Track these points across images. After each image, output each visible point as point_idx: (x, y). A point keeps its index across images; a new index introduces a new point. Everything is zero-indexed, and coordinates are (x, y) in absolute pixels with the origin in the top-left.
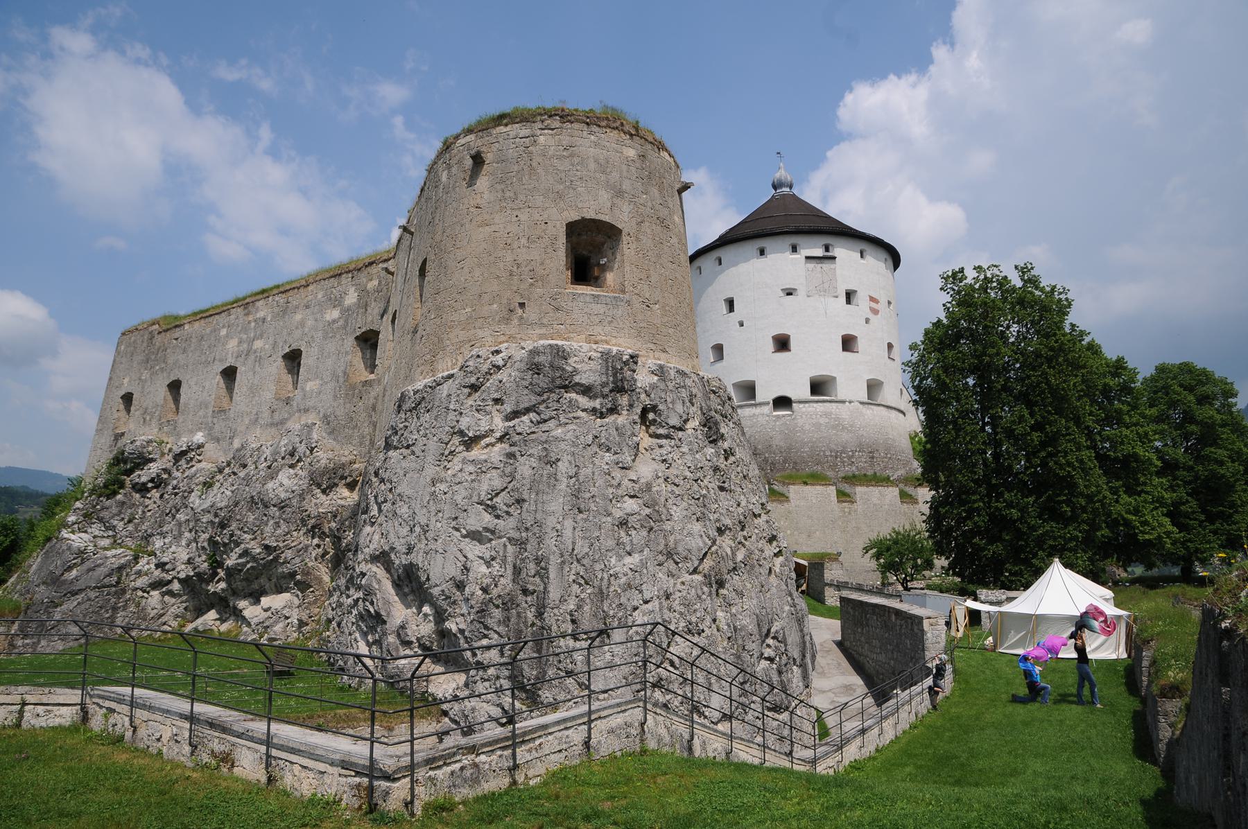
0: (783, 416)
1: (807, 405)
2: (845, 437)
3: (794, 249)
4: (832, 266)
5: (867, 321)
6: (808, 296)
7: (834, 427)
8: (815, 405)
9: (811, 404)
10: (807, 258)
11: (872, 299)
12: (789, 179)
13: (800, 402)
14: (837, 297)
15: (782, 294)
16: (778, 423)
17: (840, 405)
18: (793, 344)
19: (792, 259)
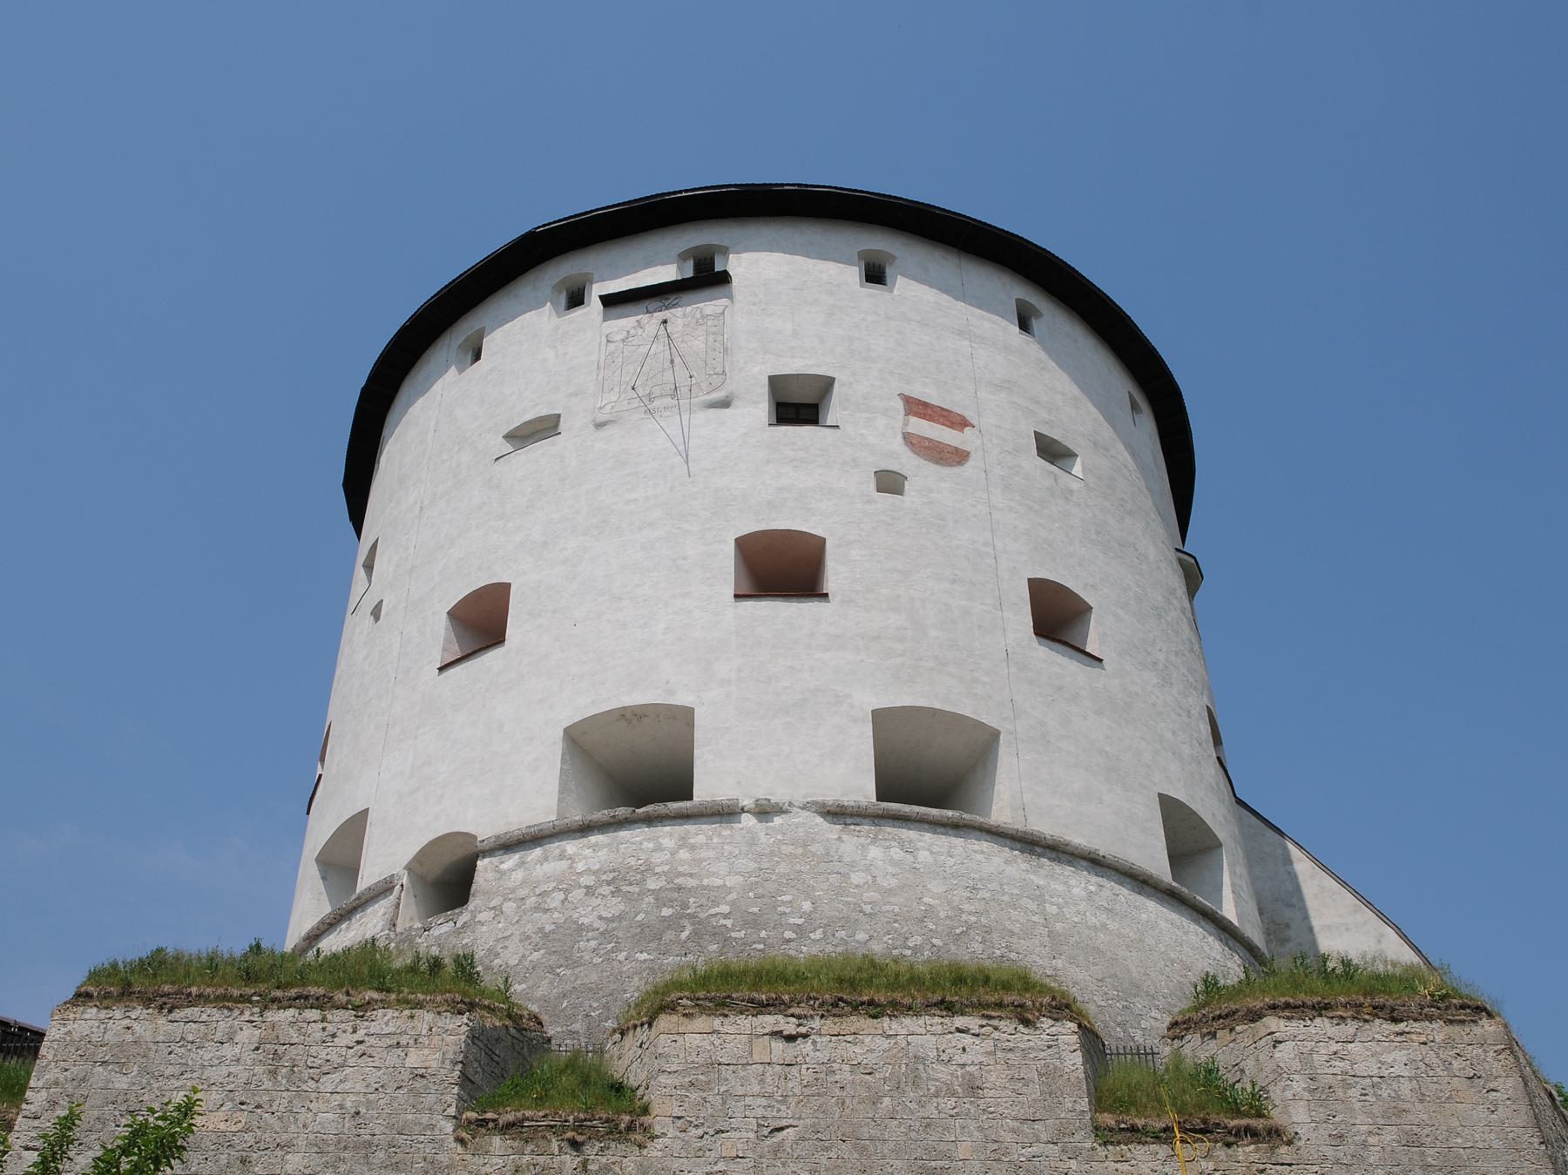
1: (537, 852)
6: (600, 425)
8: (571, 846)
9: (554, 847)
10: (609, 301)
14: (725, 404)
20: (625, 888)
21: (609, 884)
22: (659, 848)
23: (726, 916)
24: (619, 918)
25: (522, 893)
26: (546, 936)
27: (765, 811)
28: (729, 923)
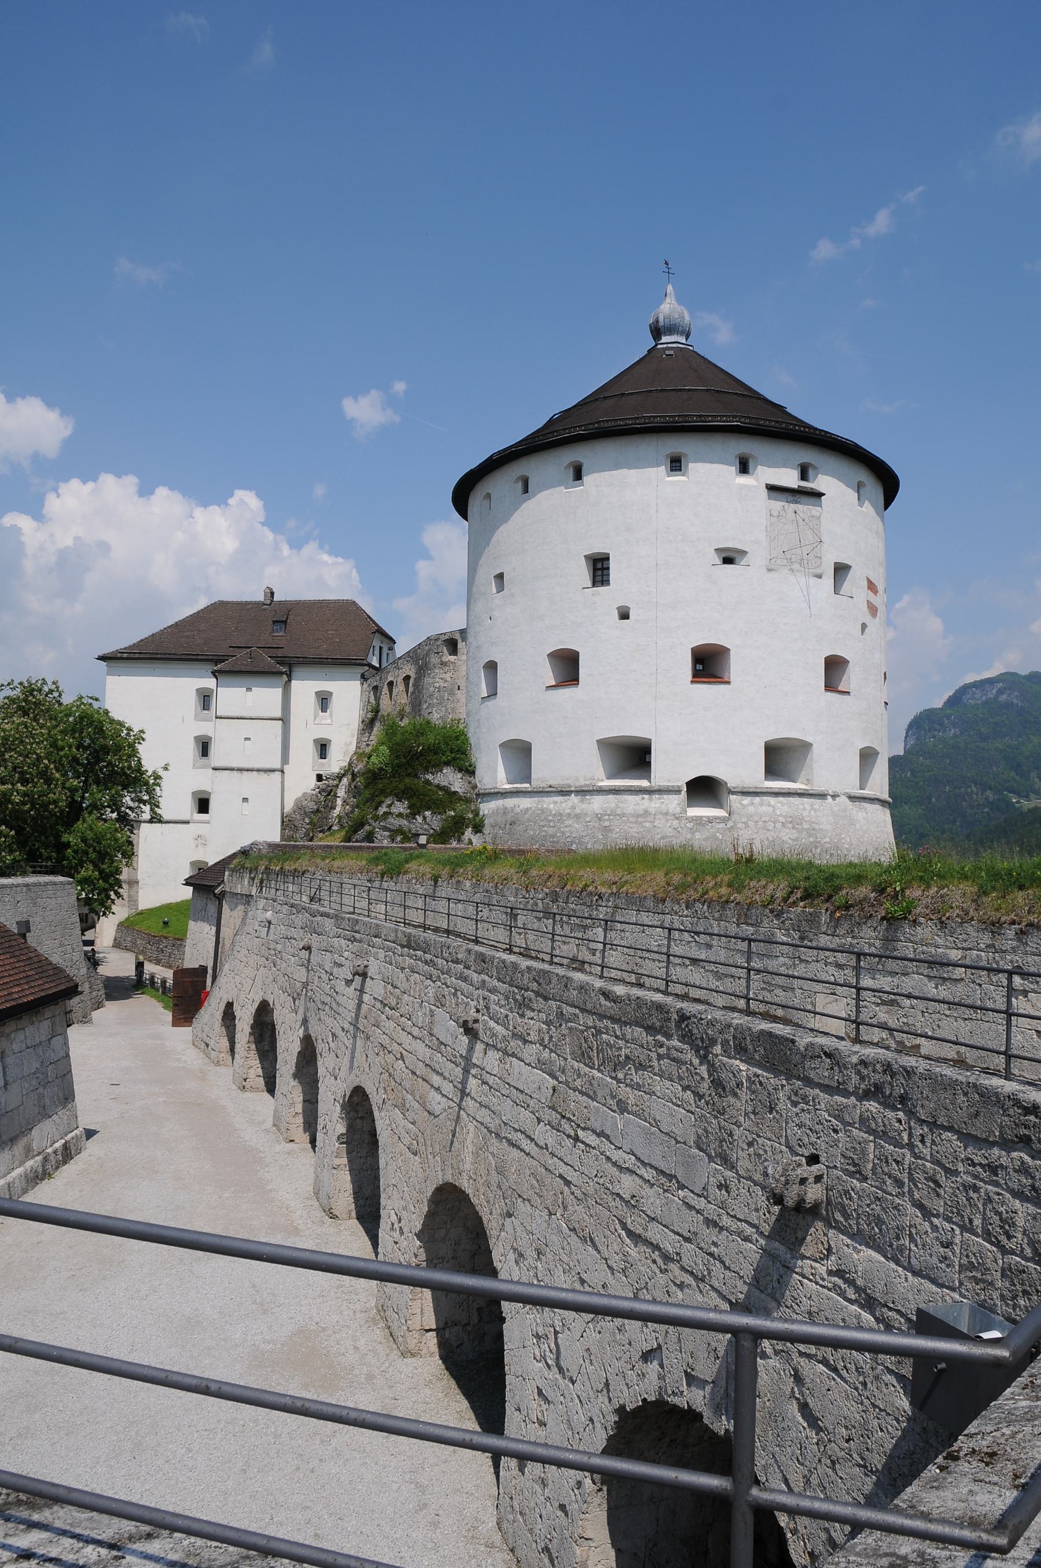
0: (710, 820)
1: (757, 800)
3: (744, 468)
4: (815, 511)
5: (864, 626)
6: (770, 570)
8: (772, 800)
10: (772, 489)
12: (687, 318)
13: (745, 793)
14: (820, 577)
15: (718, 561)
16: (698, 835)
17: (816, 802)
18: (736, 666)
19: (742, 487)
22: (805, 809)
23: (829, 843)
25: (756, 819)
27: (834, 796)
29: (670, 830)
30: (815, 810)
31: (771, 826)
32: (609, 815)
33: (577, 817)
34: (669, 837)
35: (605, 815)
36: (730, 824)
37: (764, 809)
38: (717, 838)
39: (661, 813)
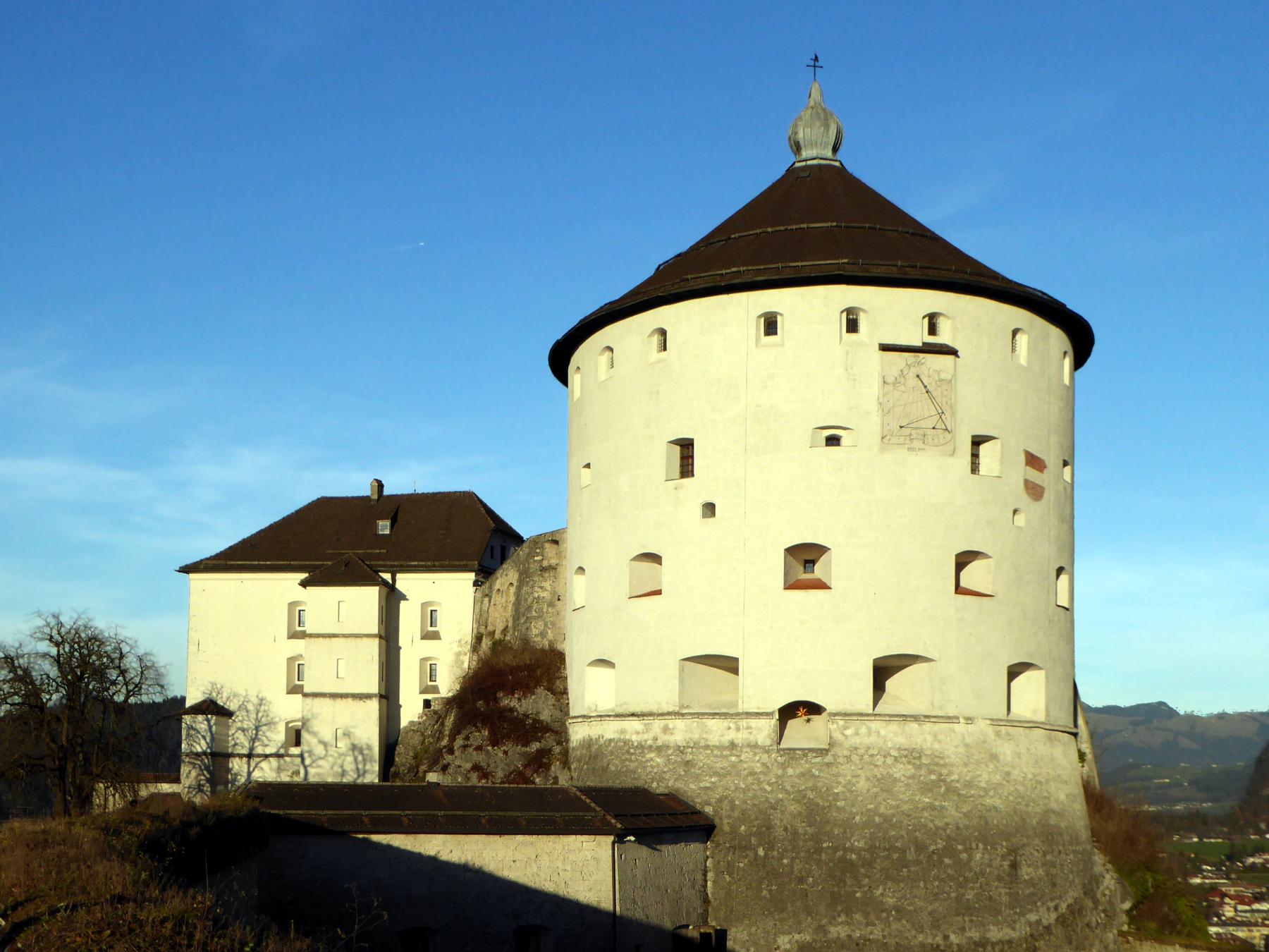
2: (953, 813)
7: (927, 788)
11: (1033, 461)
16: (790, 771)
20: (913, 761)
21: (906, 757)
23: (958, 781)
24: (912, 777)
25: (861, 751)
26: (878, 780)
28: (958, 785)
29: (758, 765)
30: (940, 742)
31: (879, 760)
32: (692, 748)
33: (659, 749)
34: (756, 773)
35: (688, 747)
36: (829, 759)
37: (872, 739)
38: (813, 776)
39: (749, 745)
